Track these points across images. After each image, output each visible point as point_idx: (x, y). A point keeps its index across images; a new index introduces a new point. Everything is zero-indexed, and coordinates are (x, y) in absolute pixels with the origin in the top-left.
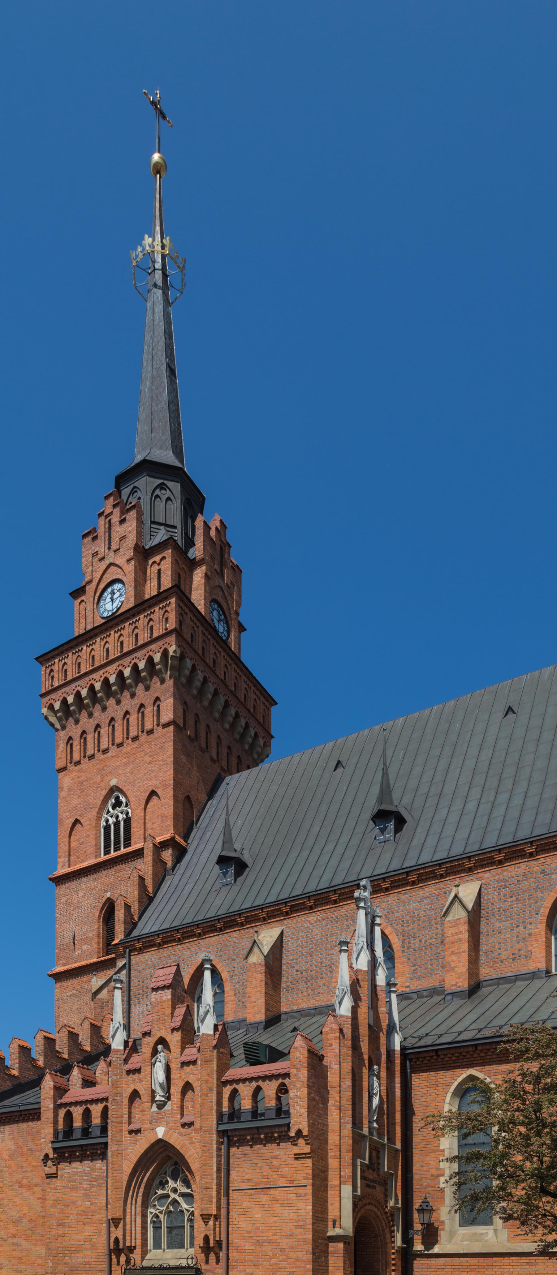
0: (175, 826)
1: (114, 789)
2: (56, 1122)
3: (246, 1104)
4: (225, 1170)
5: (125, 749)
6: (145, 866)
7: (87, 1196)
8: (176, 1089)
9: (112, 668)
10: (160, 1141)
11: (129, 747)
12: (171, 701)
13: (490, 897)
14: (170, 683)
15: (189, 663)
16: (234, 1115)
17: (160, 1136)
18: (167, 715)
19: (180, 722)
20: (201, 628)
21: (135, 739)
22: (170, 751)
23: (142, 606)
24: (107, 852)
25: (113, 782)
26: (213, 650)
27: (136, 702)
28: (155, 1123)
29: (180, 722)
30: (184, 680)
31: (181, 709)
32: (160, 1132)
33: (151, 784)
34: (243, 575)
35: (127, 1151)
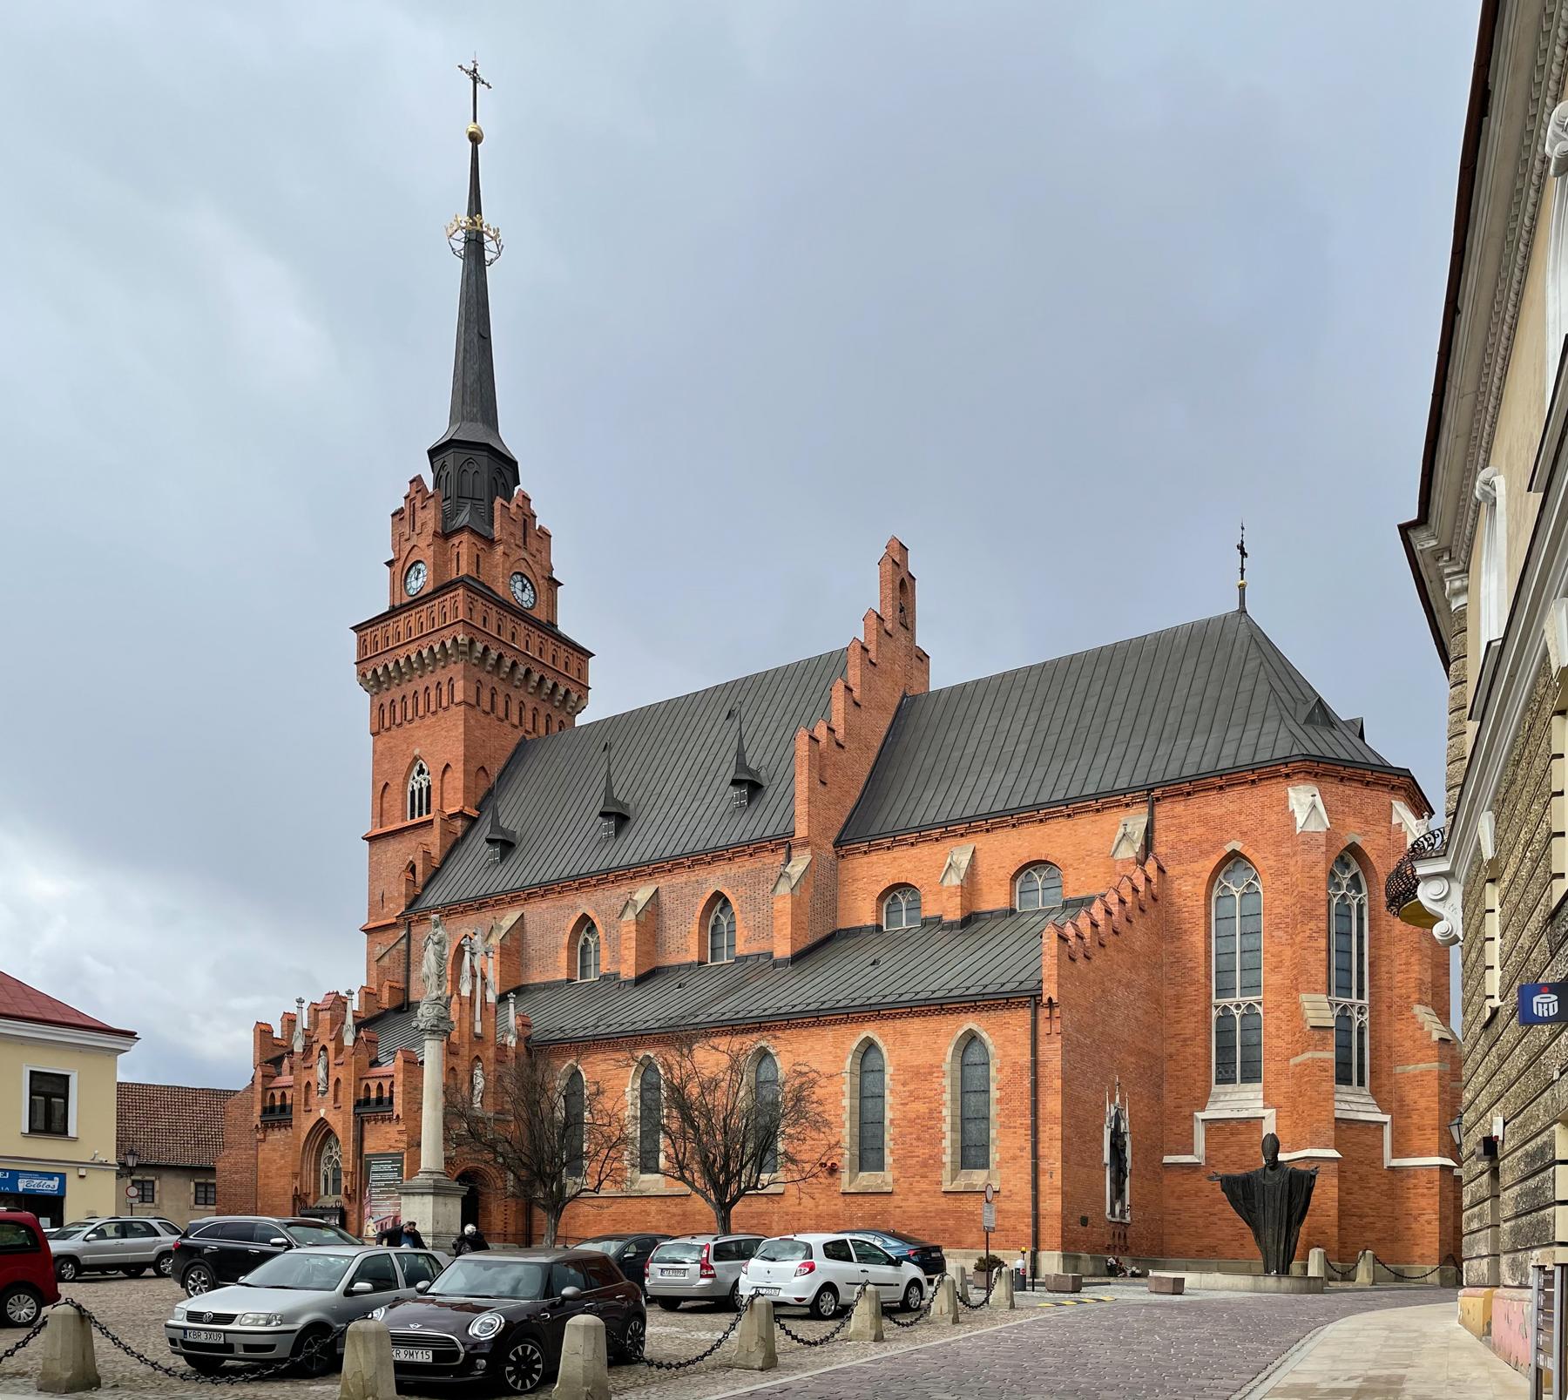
1: (416, 759)
2: (263, 1100)
4: (360, 1141)
5: (427, 721)
7: (282, 1157)
8: (332, 1082)
9: (425, 641)
11: (430, 720)
12: (461, 683)
14: (461, 665)
15: (479, 647)
16: (367, 1101)
18: (459, 697)
19: (473, 701)
21: (434, 713)
22: (461, 729)
23: (442, 589)
25: (417, 752)
26: (510, 625)
28: (319, 1105)
29: (473, 701)
32: (322, 1113)
33: (447, 758)
35: (306, 1123)
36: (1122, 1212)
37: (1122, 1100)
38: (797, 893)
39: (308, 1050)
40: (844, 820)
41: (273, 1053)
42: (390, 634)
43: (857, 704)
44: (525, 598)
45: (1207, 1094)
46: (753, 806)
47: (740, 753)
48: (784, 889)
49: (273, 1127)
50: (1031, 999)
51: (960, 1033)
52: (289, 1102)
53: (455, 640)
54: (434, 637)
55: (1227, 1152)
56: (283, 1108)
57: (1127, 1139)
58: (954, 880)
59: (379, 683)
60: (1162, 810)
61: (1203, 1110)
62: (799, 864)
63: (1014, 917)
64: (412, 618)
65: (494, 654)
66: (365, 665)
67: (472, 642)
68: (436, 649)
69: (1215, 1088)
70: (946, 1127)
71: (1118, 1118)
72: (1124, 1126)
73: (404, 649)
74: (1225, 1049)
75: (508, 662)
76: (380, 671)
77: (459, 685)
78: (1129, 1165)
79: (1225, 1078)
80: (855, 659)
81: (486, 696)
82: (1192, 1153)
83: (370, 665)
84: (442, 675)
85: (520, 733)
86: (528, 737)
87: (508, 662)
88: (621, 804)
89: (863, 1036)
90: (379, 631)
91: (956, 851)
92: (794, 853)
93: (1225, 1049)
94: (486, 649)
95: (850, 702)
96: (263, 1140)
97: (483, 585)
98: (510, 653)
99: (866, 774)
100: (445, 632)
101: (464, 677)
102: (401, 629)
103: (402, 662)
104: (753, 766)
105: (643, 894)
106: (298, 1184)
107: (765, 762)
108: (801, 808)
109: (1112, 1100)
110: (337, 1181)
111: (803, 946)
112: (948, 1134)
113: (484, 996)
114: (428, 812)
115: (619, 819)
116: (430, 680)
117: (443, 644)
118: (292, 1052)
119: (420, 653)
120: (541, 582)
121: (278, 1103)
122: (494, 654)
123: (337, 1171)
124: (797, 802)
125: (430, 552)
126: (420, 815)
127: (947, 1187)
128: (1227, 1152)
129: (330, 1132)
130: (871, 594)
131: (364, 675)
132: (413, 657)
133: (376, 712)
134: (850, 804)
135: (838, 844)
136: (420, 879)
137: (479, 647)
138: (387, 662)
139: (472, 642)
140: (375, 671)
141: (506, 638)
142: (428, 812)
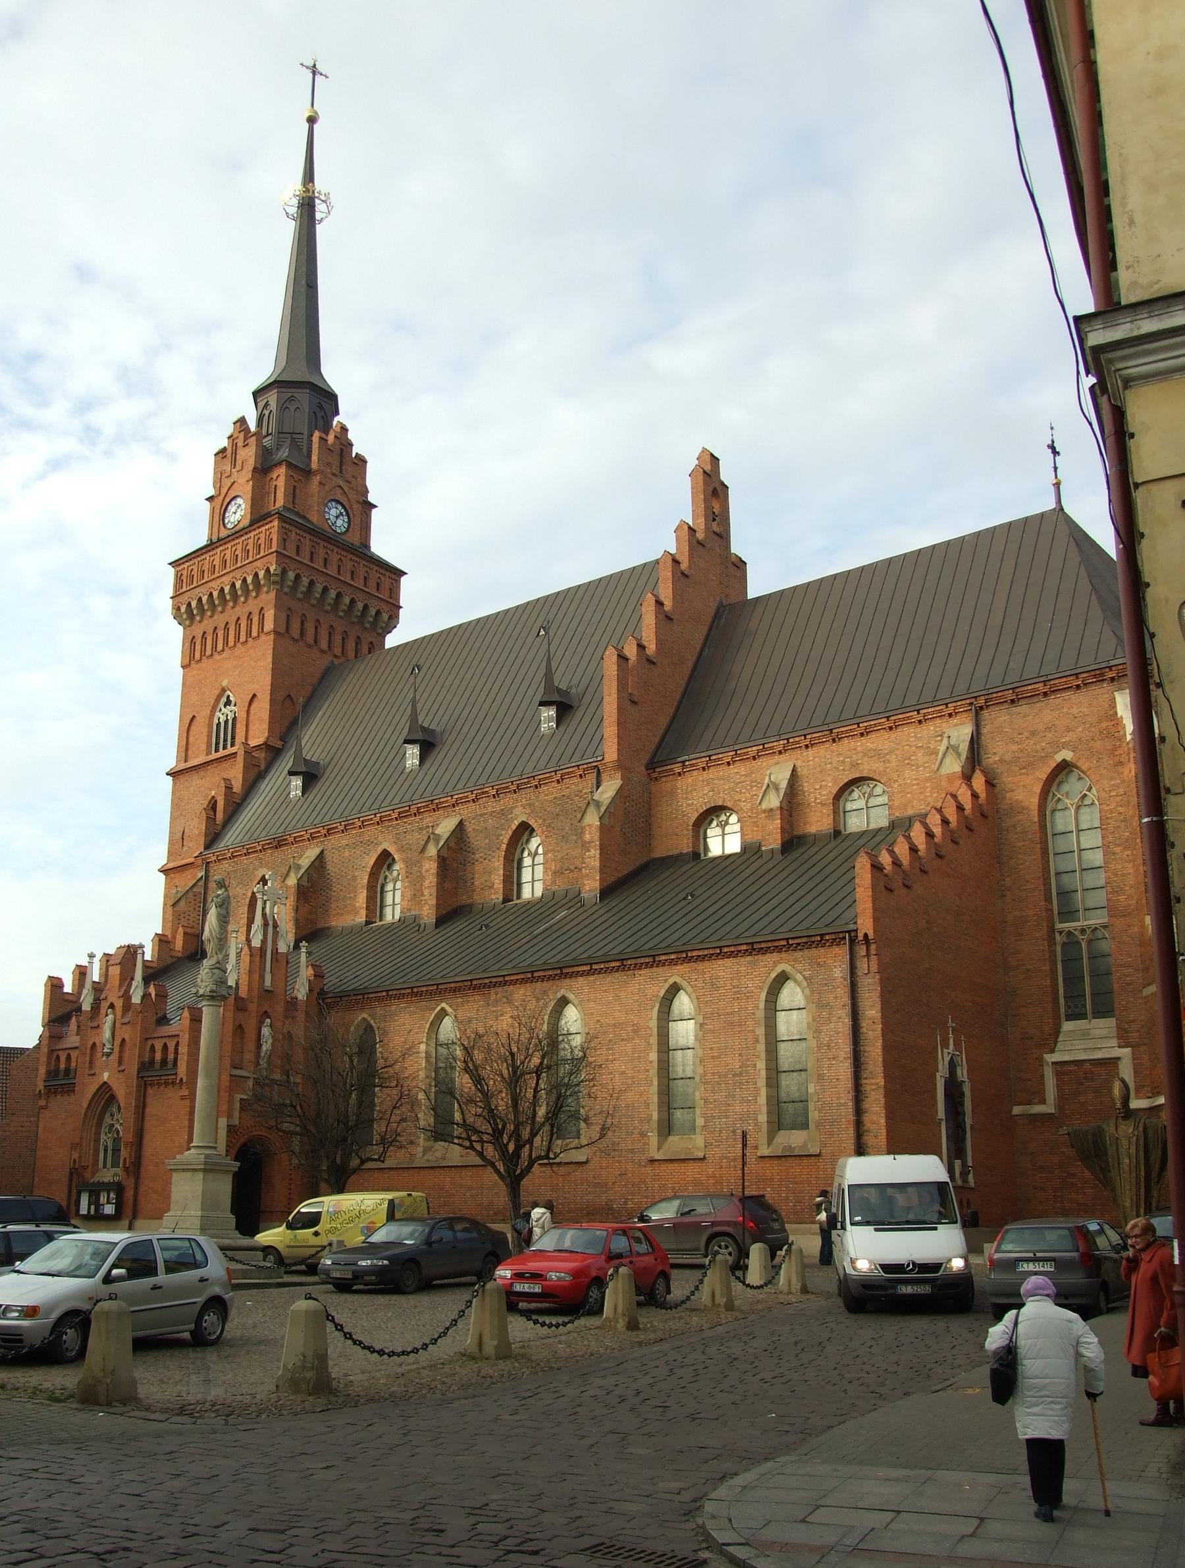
0: (270, 729)
3: (158, 1056)
6: (236, 773)
10: (105, 1083)
12: (272, 612)
13: (469, 827)
14: (273, 594)
17: (105, 1079)
18: (269, 625)
20: (309, 537)
22: (270, 659)
24: (225, 748)
27: (246, 610)
29: (282, 630)
30: (286, 590)
31: (284, 616)
34: (368, 465)
36: (964, 1174)
37: (957, 1046)
38: (606, 821)
39: (96, 1007)
40: (657, 740)
41: (62, 1008)
42: (206, 568)
43: (669, 618)
44: (341, 524)
45: (1057, 1032)
46: (562, 728)
47: (549, 675)
48: (592, 819)
49: (56, 1092)
50: (852, 938)
51: (773, 975)
52: (73, 1065)
53: (268, 570)
54: (248, 569)
55: (1082, 1099)
56: (67, 1071)
57: (967, 1089)
58: (774, 801)
59: (191, 616)
60: (998, 719)
61: (1052, 1051)
62: (609, 789)
63: (840, 839)
64: (228, 551)
65: (305, 581)
66: (180, 599)
67: (284, 572)
68: (249, 580)
69: (1067, 1026)
70: (762, 1082)
71: (952, 1065)
72: (962, 1074)
73: (219, 581)
74: (1074, 980)
75: (319, 588)
76: (194, 604)
77: (270, 615)
78: (968, 1121)
79: (1075, 1015)
80: (666, 574)
81: (296, 625)
82: (1043, 1101)
83: (185, 599)
84: (253, 605)
85: (326, 660)
86: (336, 662)
87: (319, 588)
88: (424, 729)
89: (671, 981)
90: (194, 566)
91: (774, 769)
92: (604, 776)
93: (1074, 980)
94: (298, 577)
95: (662, 617)
96: (45, 1108)
97: (298, 514)
98: (321, 579)
99: (681, 690)
100: (258, 563)
101: (276, 607)
102: (217, 563)
103: (215, 594)
104: (563, 686)
105: (446, 827)
106: (76, 1155)
107: (575, 681)
108: (610, 730)
109: (945, 1045)
110: (116, 1151)
111: (613, 879)
112: (763, 1091)
113: (275, 943)
114: (233, 745)
115: (427, 747)
116: (241, 611)
117: (256, 575)
118: (79, 1009)
119: (233, 585)
120: (355, 506)
121: (62, 1066)
122: (305, 581)
123: (117, 1141)
124: (606, 722)
125: (249, 487)
126: (225, 748)
127: (764, 1151)
128: (1082, 1099)
129: (112, 1098)
130: (681, 505)
131: (179, 609)
132: (227, 589)
133: (188, 644)
134: (664, 722)
135: (652, 765)
136: (220, 815)
137: (291, 575)
138: (201, 594)
139: (284, 572)
140: (189, 604)
141: (318, 564)
142: (233, 745)
